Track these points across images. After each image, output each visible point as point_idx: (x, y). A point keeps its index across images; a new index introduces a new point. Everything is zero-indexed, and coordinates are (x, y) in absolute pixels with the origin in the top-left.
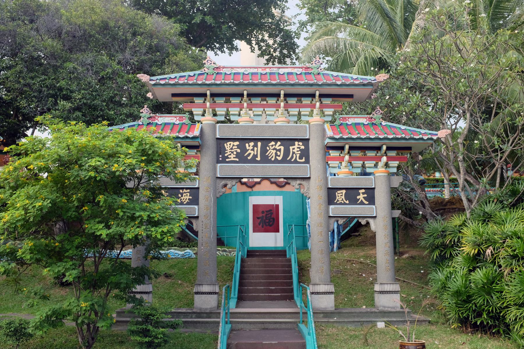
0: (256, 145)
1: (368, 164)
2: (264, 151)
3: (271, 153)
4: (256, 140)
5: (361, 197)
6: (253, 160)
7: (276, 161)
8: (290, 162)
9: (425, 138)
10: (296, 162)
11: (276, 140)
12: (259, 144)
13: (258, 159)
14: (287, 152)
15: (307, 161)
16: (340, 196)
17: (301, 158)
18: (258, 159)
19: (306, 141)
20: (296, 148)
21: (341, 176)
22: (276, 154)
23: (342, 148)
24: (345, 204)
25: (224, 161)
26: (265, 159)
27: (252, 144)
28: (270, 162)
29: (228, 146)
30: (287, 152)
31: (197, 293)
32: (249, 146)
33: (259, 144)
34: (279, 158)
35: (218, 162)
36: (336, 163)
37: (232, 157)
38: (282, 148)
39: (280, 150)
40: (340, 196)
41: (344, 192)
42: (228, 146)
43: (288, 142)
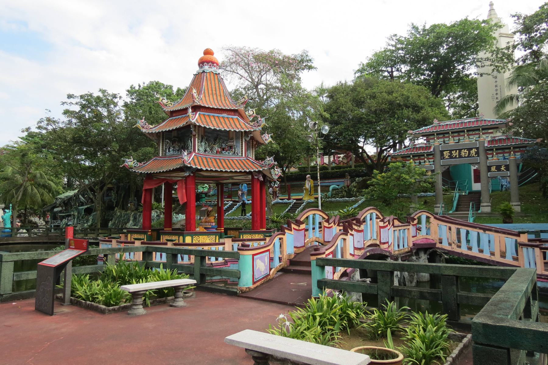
0: (456, 152)
1: (506, 155)
2: (460, 153)
3: (463, 154)
4: (456, 150)
5: (503, 168)
6: (456, 157)
7: (465, 157)
8: (471, 157)
9: (530, 143)
10: (473, 157)
11: (465, 149)
12: (458, 151)
13: (457, 157)
14: (469, 153)
15: (478, 156)
16: (493, 169)
17: (475, 155)
18: (457, 157)
19: (477, 148)
20: (473, 151)
21: (494, 161)
22: (465, 154)
23: (492, 150)
24: (495, 172)
25: (444, 159)
26: (460, 157)
27: (455, 151)
28: (462, 157)
29: (445, 153)
30: (469, 153)
31: (435, 207)
32: (453, 152)
33: (458, 151)
34: (466, 156)
35: (441, 159)
36: (491, 156)
37: (447, 157)
38: (467, 152)
39: (466, 153)
40: (493, 169)
41: (495, 167)
42: (445, 153)
43: (470, 150)
